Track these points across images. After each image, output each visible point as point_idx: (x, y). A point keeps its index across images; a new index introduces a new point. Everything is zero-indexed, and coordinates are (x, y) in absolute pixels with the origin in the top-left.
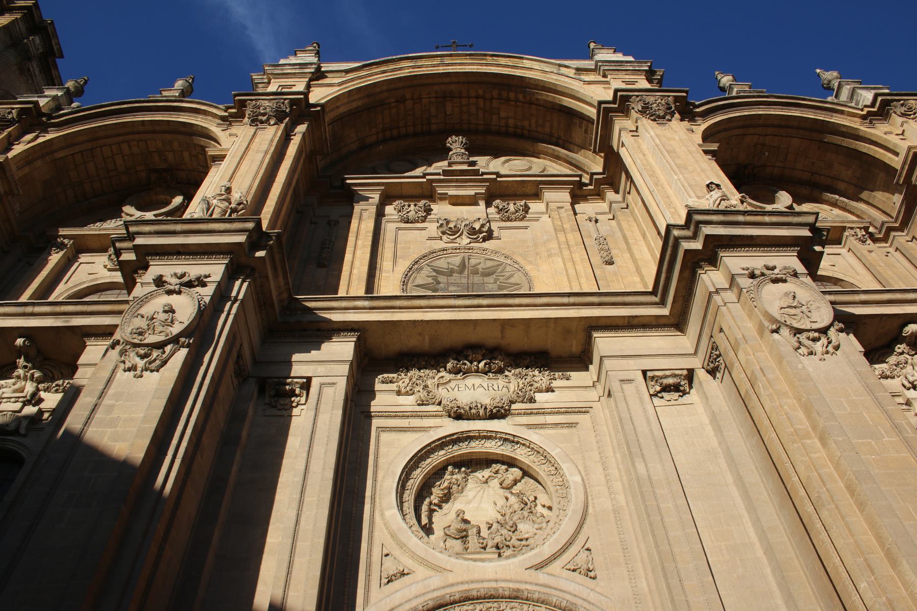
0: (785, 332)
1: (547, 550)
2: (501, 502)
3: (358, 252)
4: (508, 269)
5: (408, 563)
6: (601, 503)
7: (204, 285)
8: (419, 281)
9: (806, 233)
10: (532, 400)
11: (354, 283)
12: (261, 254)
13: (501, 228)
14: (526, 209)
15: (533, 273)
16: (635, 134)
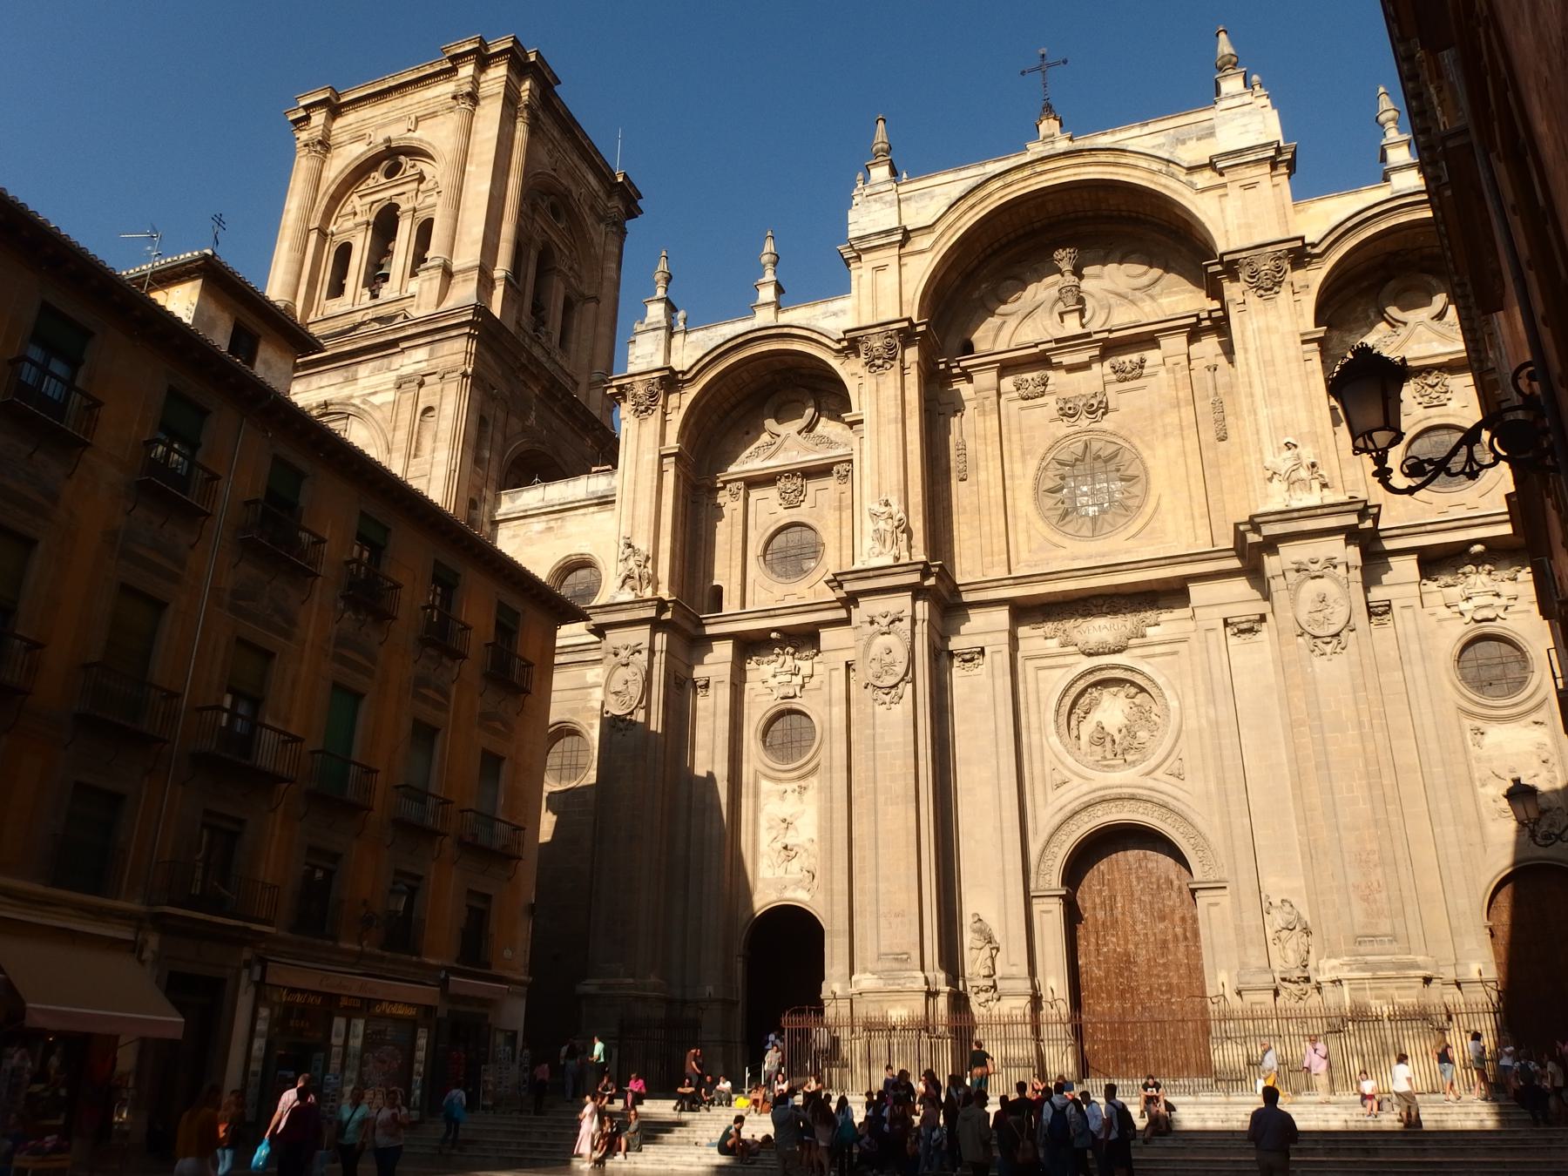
0: (1307, 637)
1: (1153, 762)
2: (1127, 710)
3: (991, 464)
4: (1127, 456)
5: (1068, 774)
6: (1191, 723)
7: (900, 620)
8: (1050, 484)
9: (1352, 519)
10: (1143, 636)
11: (994, 510)
12: (931, 581)
13: (1119, 392)
14: (1143, 361)
15: (1150, 463)
16: (1242, 307)
